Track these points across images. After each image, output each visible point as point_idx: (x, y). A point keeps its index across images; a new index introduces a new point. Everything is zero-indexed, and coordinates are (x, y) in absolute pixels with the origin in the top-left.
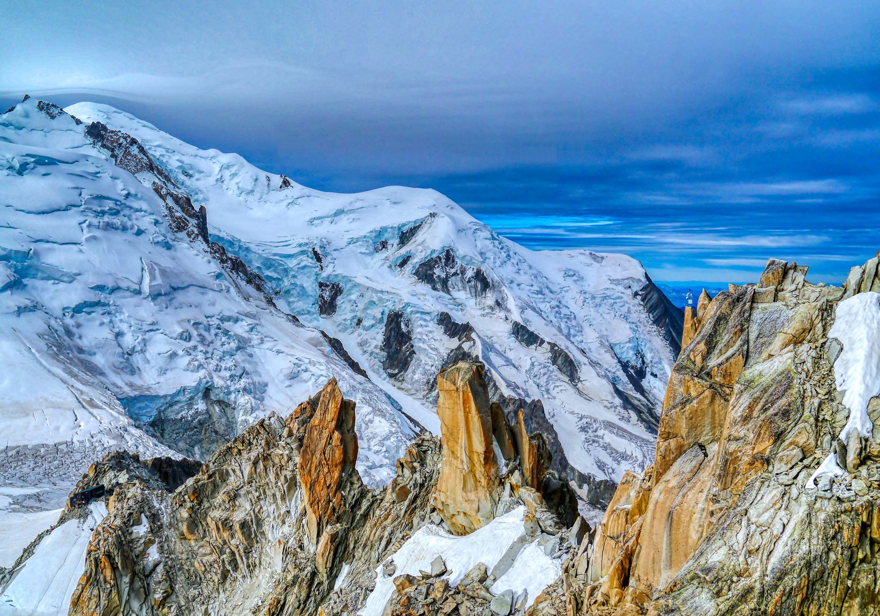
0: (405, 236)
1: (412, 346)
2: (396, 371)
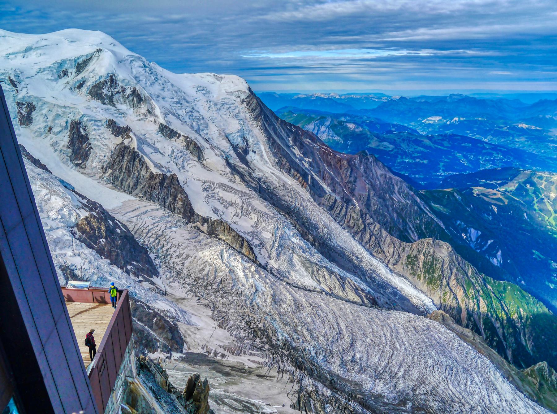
0: (81, 66)
1: (90, 144)
2: (80, 162)
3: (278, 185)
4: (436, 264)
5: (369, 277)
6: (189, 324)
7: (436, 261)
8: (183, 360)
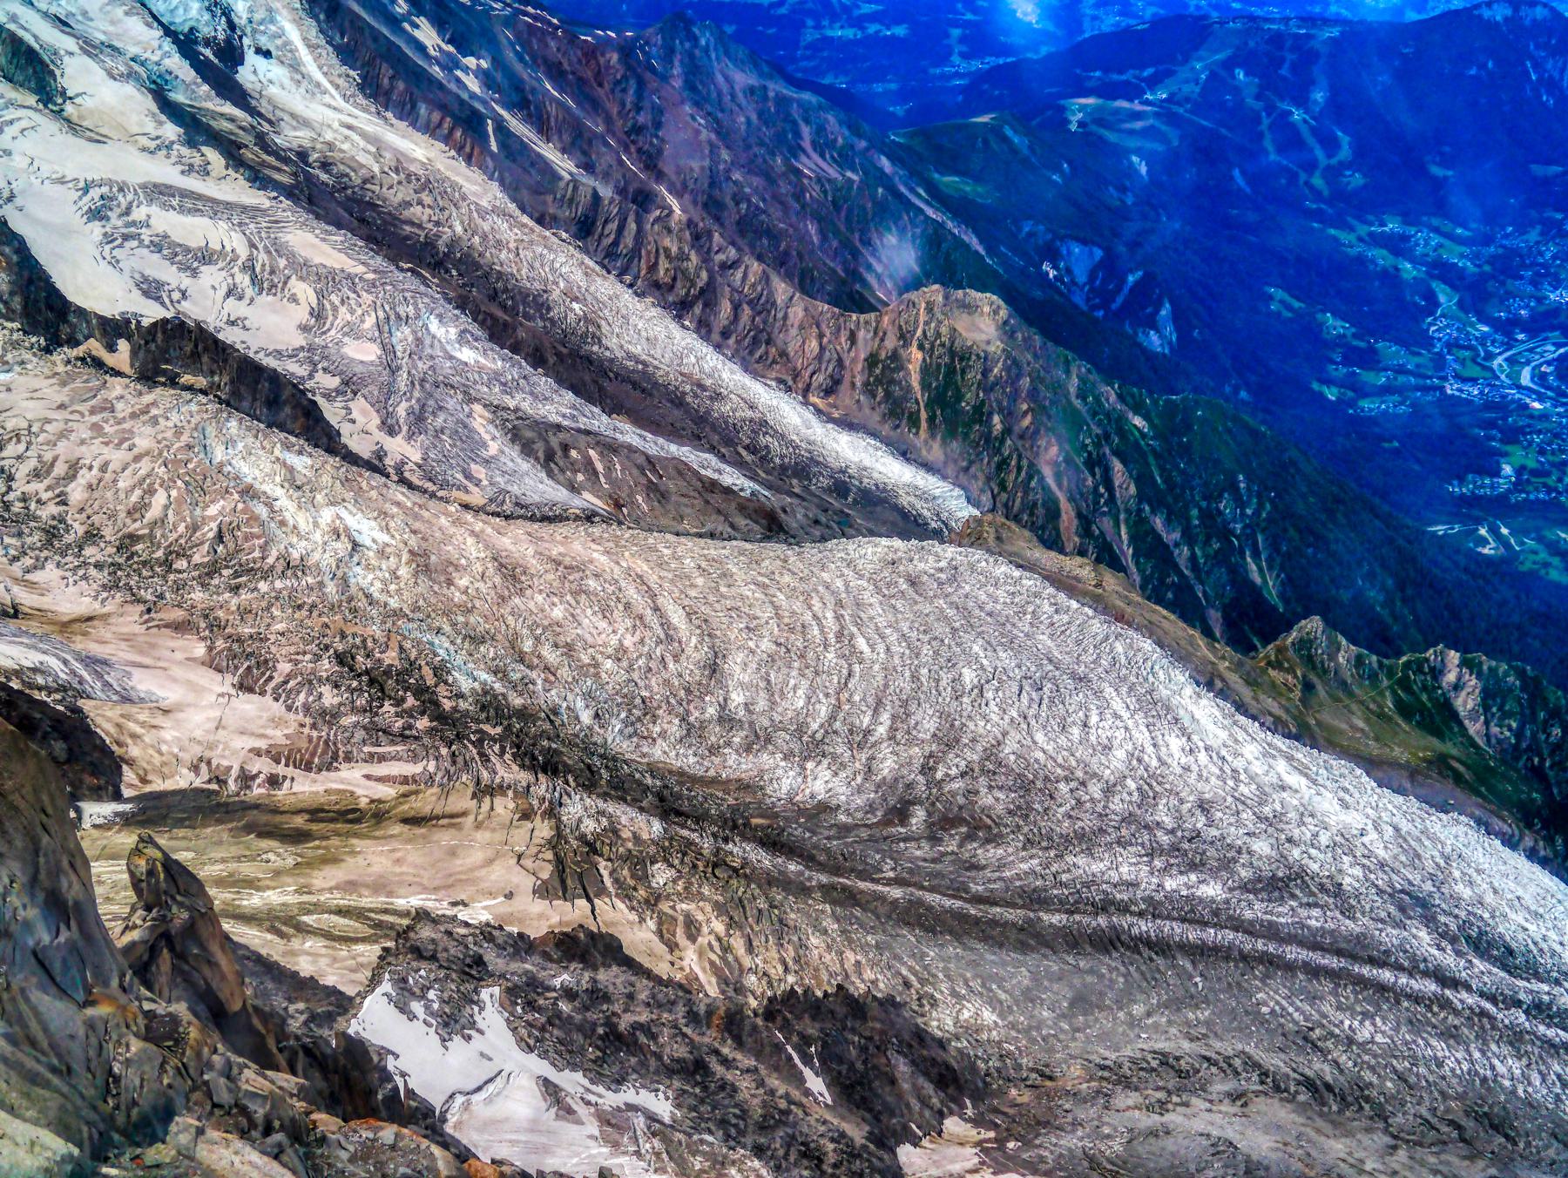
3: (376, 169)
4: (963, 372)
5: (747, 448)
6: (126, 699)
7: (961, 359)
8: (127, 821)
